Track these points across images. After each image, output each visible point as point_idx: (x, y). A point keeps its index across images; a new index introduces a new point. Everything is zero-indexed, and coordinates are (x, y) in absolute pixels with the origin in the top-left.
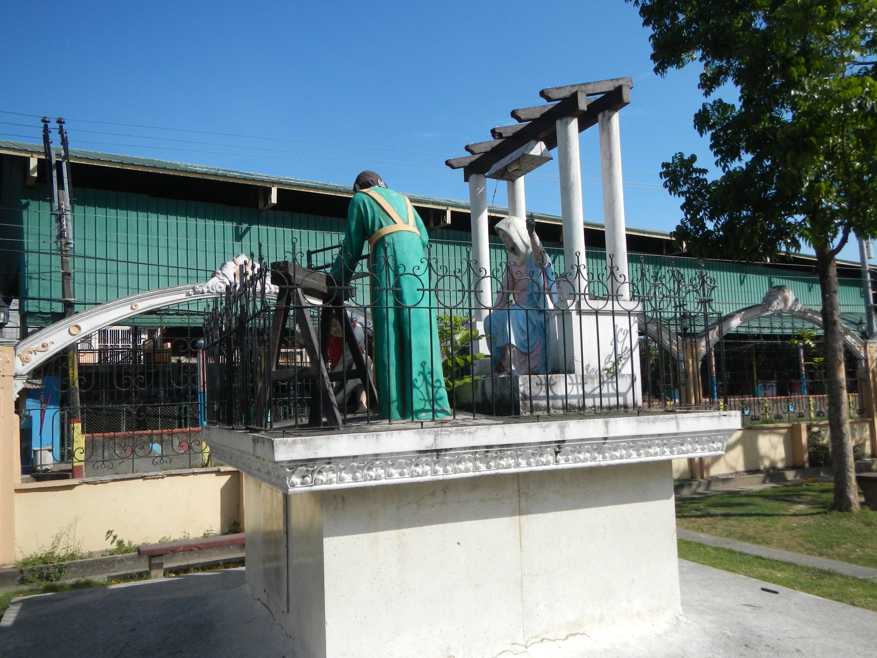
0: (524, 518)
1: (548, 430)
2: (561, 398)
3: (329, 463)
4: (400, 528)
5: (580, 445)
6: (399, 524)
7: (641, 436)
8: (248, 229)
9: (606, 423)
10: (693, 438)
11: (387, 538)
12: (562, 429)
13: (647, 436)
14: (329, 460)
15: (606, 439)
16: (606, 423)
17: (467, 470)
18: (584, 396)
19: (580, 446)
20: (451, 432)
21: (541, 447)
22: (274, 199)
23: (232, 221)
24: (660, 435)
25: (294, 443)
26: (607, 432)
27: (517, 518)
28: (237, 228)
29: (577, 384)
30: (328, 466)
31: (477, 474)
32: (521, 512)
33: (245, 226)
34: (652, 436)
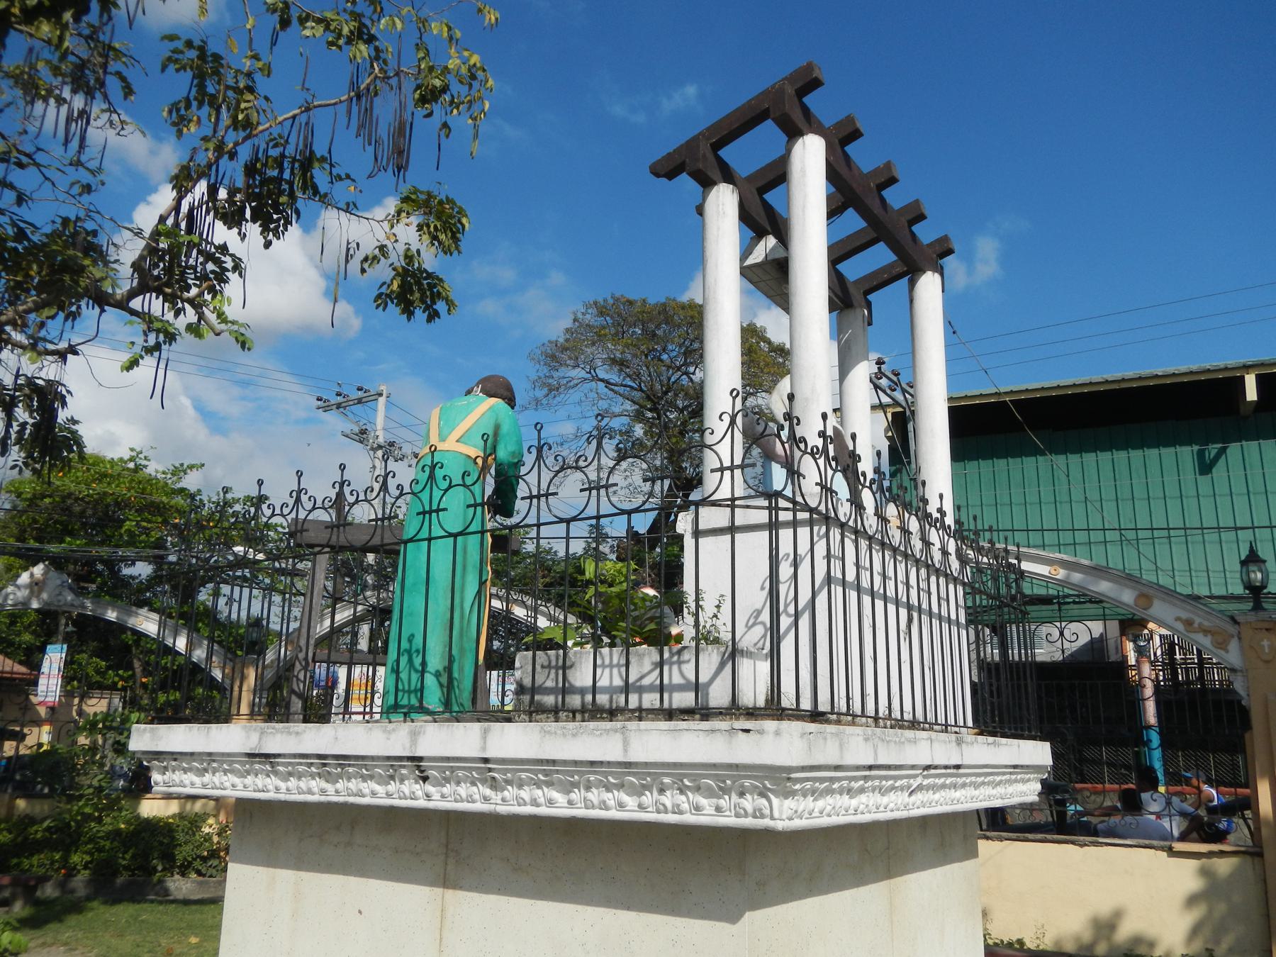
0: (450, 894)
1: (393, 736)
2: (582, 691)
3: (175, 760)
4: (299, 868)
5: (452, 767)
6: (300, 863)
7: (554, 762)
8: (1222, 451)
9: (485, 732)
10: (680, 778)
11: (286, 877)
12: (414, 735)
13: (565, 763)
14: (175, 756)
15: (486, 760)
16: (485, 732)
17: (310, 792)
18: (627, 689)
19: (452, 769)
20: (277, 731)
21: (394, 765)
22: (1252, 394)
23: (1189, 443)
24: (592, 763)
25: (145, 730)
26: (484, 749)
27: (439, 891)
28: (1201, 454)
29: (618, 665)
30: (174, 763)
31: (323, 799)
32: (446, 882)
33: (1213, 449)
34: (576, 763)
